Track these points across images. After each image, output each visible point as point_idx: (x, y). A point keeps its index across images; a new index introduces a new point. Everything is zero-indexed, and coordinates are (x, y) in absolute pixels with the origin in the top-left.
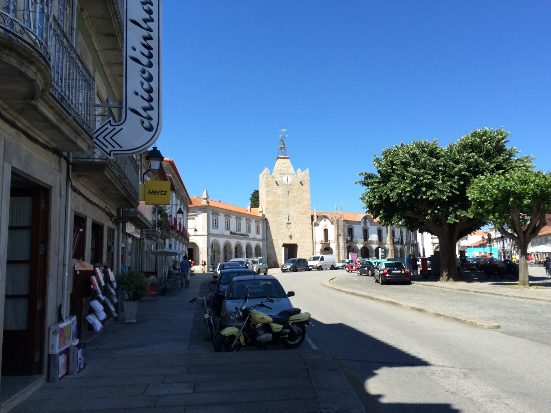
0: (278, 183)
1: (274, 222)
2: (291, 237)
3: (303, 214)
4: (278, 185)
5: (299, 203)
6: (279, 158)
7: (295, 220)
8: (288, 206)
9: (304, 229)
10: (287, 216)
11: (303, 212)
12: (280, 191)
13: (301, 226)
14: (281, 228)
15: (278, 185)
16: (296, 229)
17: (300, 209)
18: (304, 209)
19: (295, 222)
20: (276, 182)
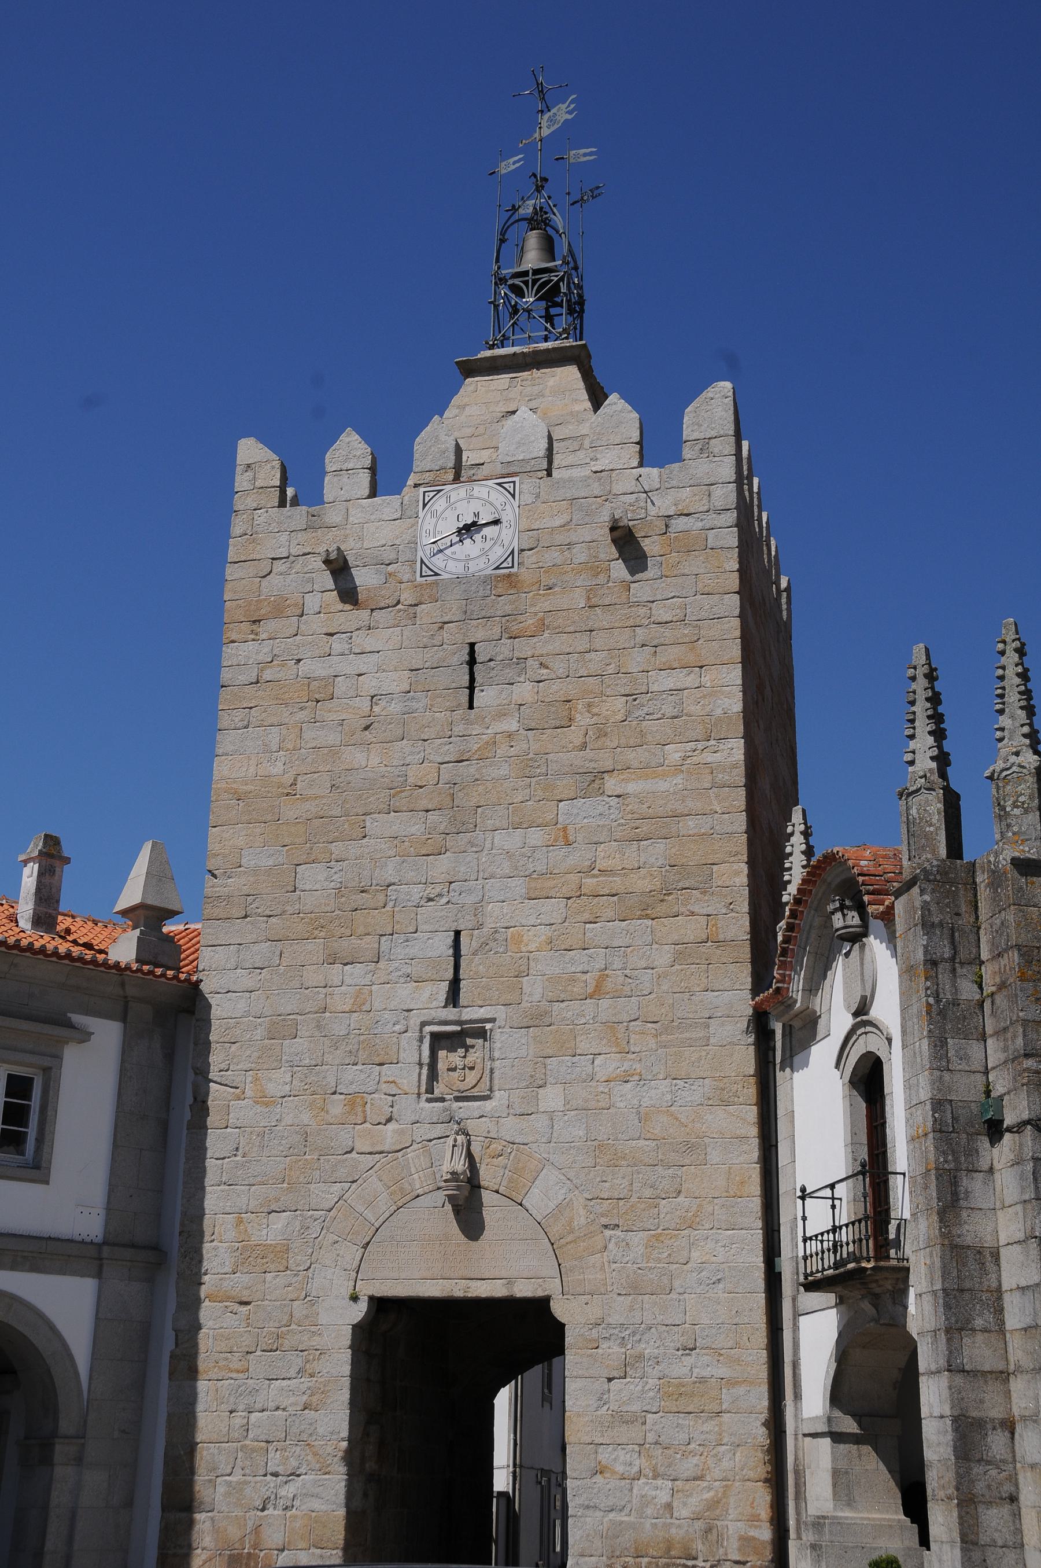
0: (363, 578)
1: (282, 1029)
2: (467, 1206)
3: (647, 908)
4: (349, 595)
5: (593, 781)
6: (470, 369)
7: (534, 989)
8: (456, 819)
9: (658, 1092)
10: (443, 945)
11: (642, 883)
12: (378, 661)
13: (608, 1065)
14: (356, 1102)
15: (349, 595)
16: (551, 1098)
17: (607, 856)
18: (656, 853)
19: (536, 1020)
20: (339, 568)
